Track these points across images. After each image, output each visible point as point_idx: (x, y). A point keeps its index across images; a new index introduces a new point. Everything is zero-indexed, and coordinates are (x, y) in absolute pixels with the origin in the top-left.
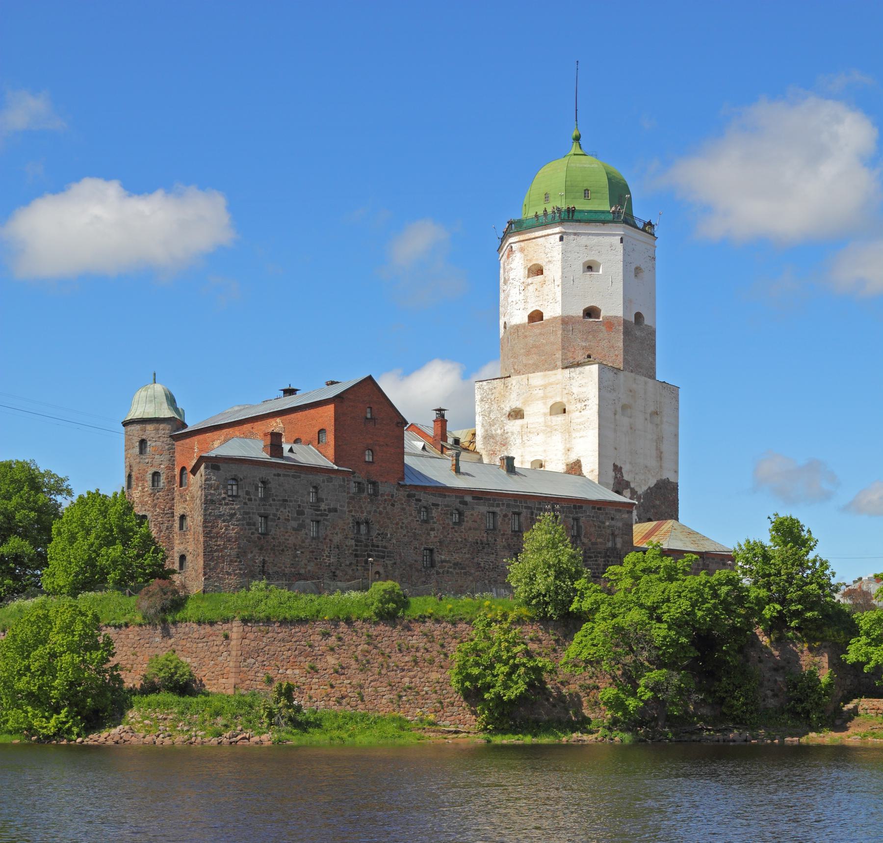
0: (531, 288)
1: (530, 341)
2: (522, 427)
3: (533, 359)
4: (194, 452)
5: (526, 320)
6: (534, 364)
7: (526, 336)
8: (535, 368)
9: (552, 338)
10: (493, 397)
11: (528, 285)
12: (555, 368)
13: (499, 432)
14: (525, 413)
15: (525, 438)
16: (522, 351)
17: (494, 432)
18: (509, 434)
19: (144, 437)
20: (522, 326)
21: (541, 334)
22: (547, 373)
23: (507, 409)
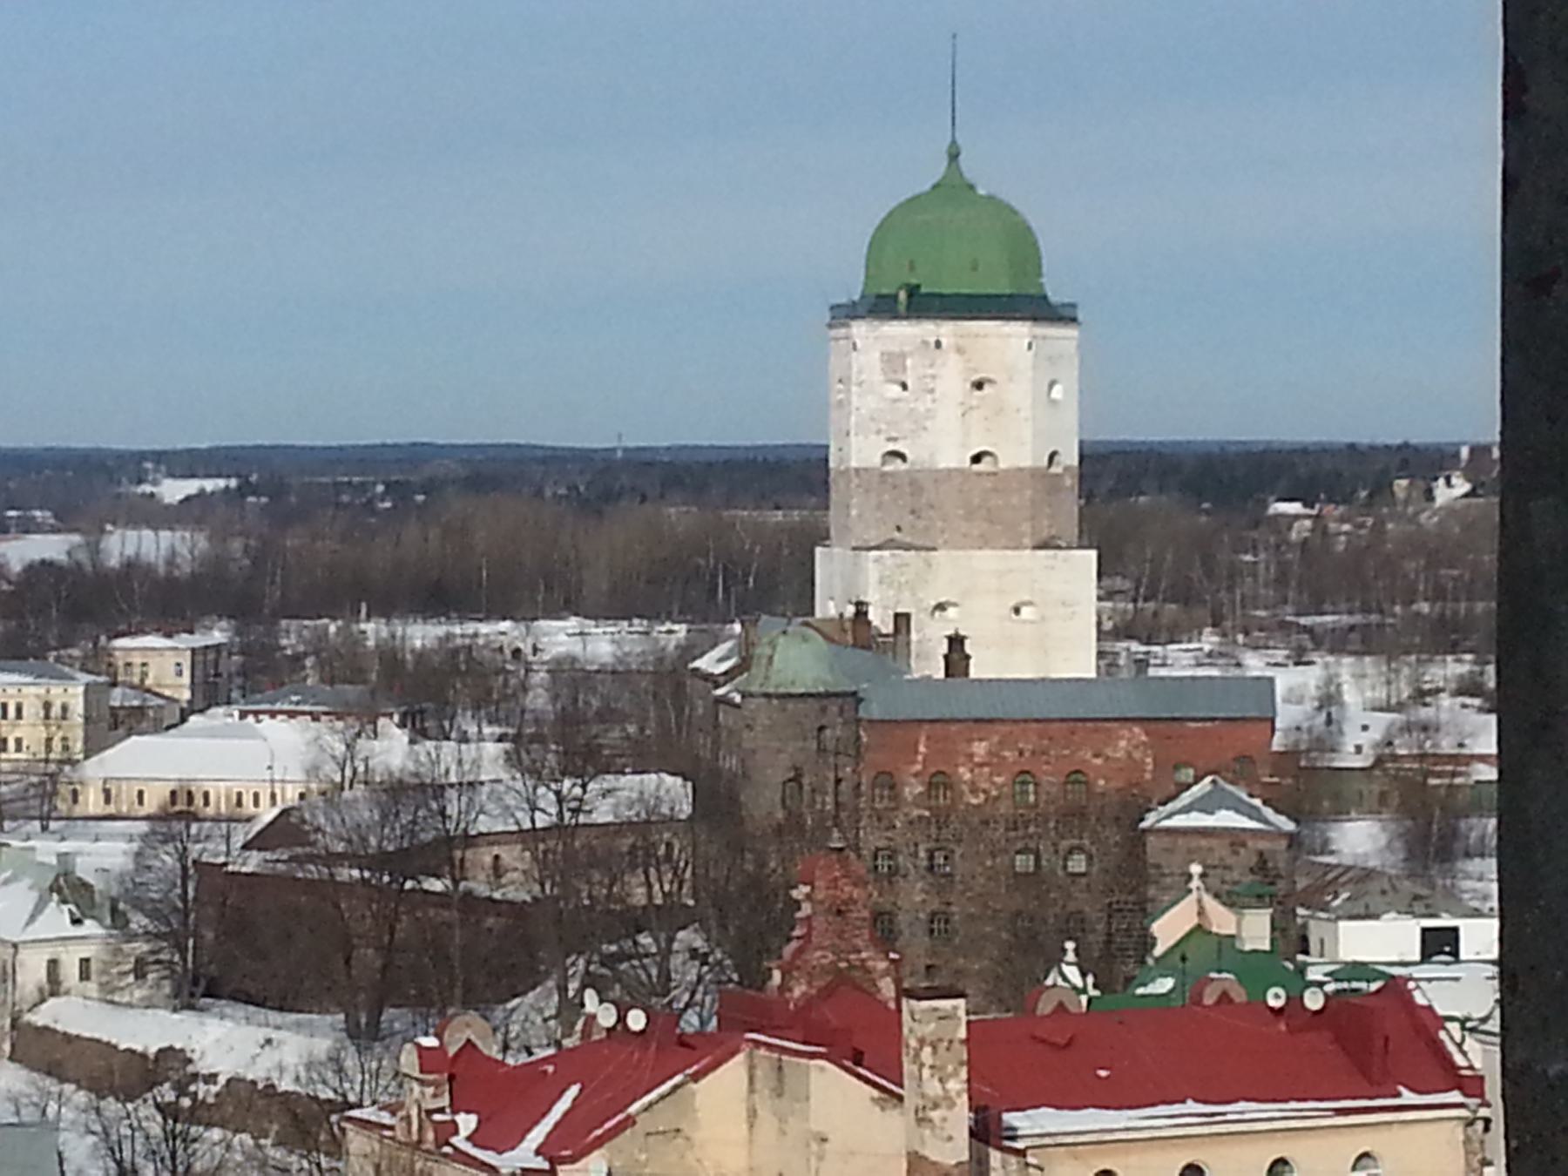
0: (975, 414)
4: (917, 752)
16: (961, 512)
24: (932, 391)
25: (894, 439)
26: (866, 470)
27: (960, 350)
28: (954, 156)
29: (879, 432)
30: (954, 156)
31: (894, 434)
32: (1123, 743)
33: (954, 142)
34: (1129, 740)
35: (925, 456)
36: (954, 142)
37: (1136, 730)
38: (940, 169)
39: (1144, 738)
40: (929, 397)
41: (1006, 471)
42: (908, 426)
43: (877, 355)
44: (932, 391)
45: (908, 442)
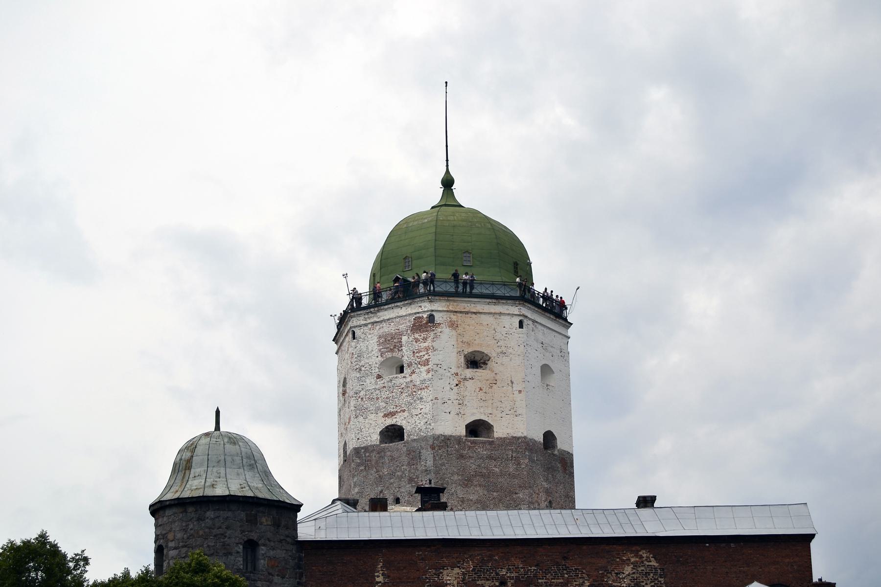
0: (469, 384)
1: (472, 465)
3: (476, 493)
6: (478, 501)
7: (462, 456)
9: (511, 468)
11: (465, 379)
16: (456, 477)
19: (254, 536)
20: (458, 440)
21: (490, 457)
24: (426, 363)
25: (392, 414)
26: (366, 449)
27: (453, 325)
28: (448, 183)
29: (378, 409)
30: (448, 183)
31: (391, 409)
32: (628, 570)
33: (447, 171)
34: (635, 565)
35: (421, 424)
36: (447, 171)
37: (644, 554)
38: (436, 194)
39: (654, 563)
40: (424, 369)
41: (503, 440)
42: (405, 398)
43: (375, 339)
44: (426, 363)
45: (406, 414)
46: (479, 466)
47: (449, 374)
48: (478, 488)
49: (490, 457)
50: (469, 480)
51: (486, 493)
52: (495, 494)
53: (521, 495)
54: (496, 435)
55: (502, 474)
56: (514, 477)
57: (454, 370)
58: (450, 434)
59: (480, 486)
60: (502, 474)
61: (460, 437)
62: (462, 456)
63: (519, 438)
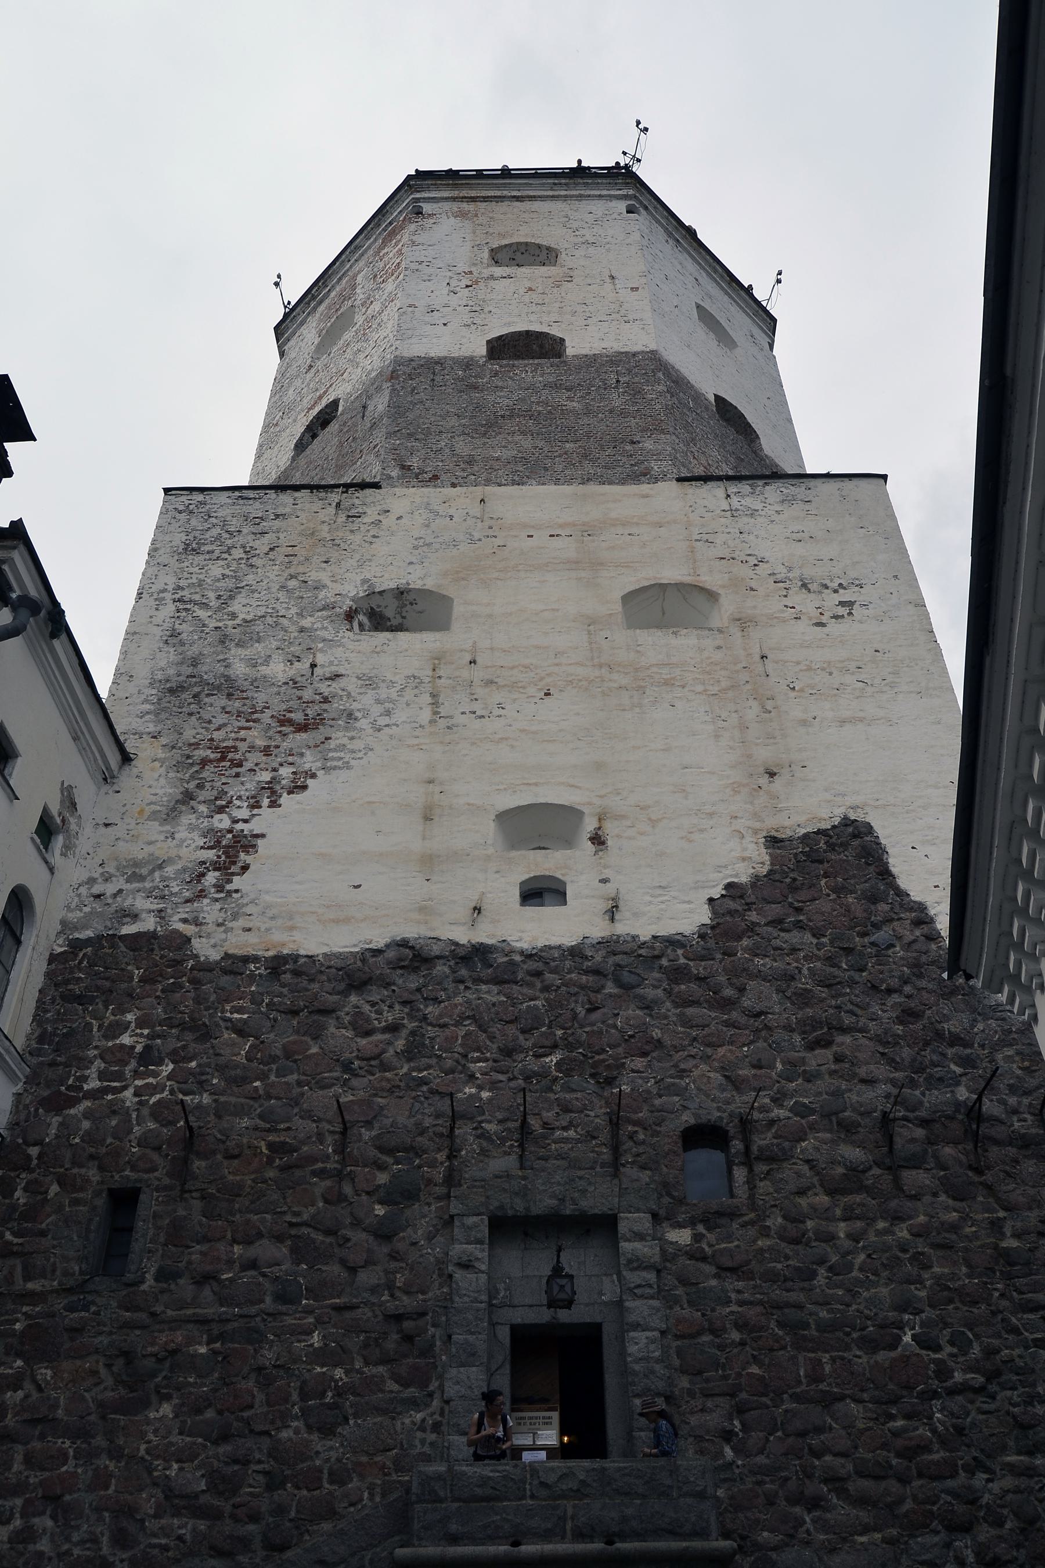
2: (437, 661)
5: (483, 351)
7: (475, 387)
8: (527, 470)
9: (617, 400)
10: (261, 545)
12: (640, 475)
13: (278, 670)
14: (458, 609)
15: (454, 704)
16: (453, 421)
17: (239, 669)
18: (351, 684)
20: (467, 363)
22: (593, 488)
23: (348, 586)
41: (590, 361)
46: (523, 400)
47: (449, 274)
48: (517, 438)
49: (556, 386)
50: (490, 425)
51: (541, 444)
52: (568, 445)
53: (648, 445)
54: (570, 351)
55: (588, 412)
56: (623, 414)
57: (462, 267)
58: (442, 355)
59: (523, 433)
60: (588, 412)
61: (472, 358)
62: (475, 387)
63: (634, 355)
